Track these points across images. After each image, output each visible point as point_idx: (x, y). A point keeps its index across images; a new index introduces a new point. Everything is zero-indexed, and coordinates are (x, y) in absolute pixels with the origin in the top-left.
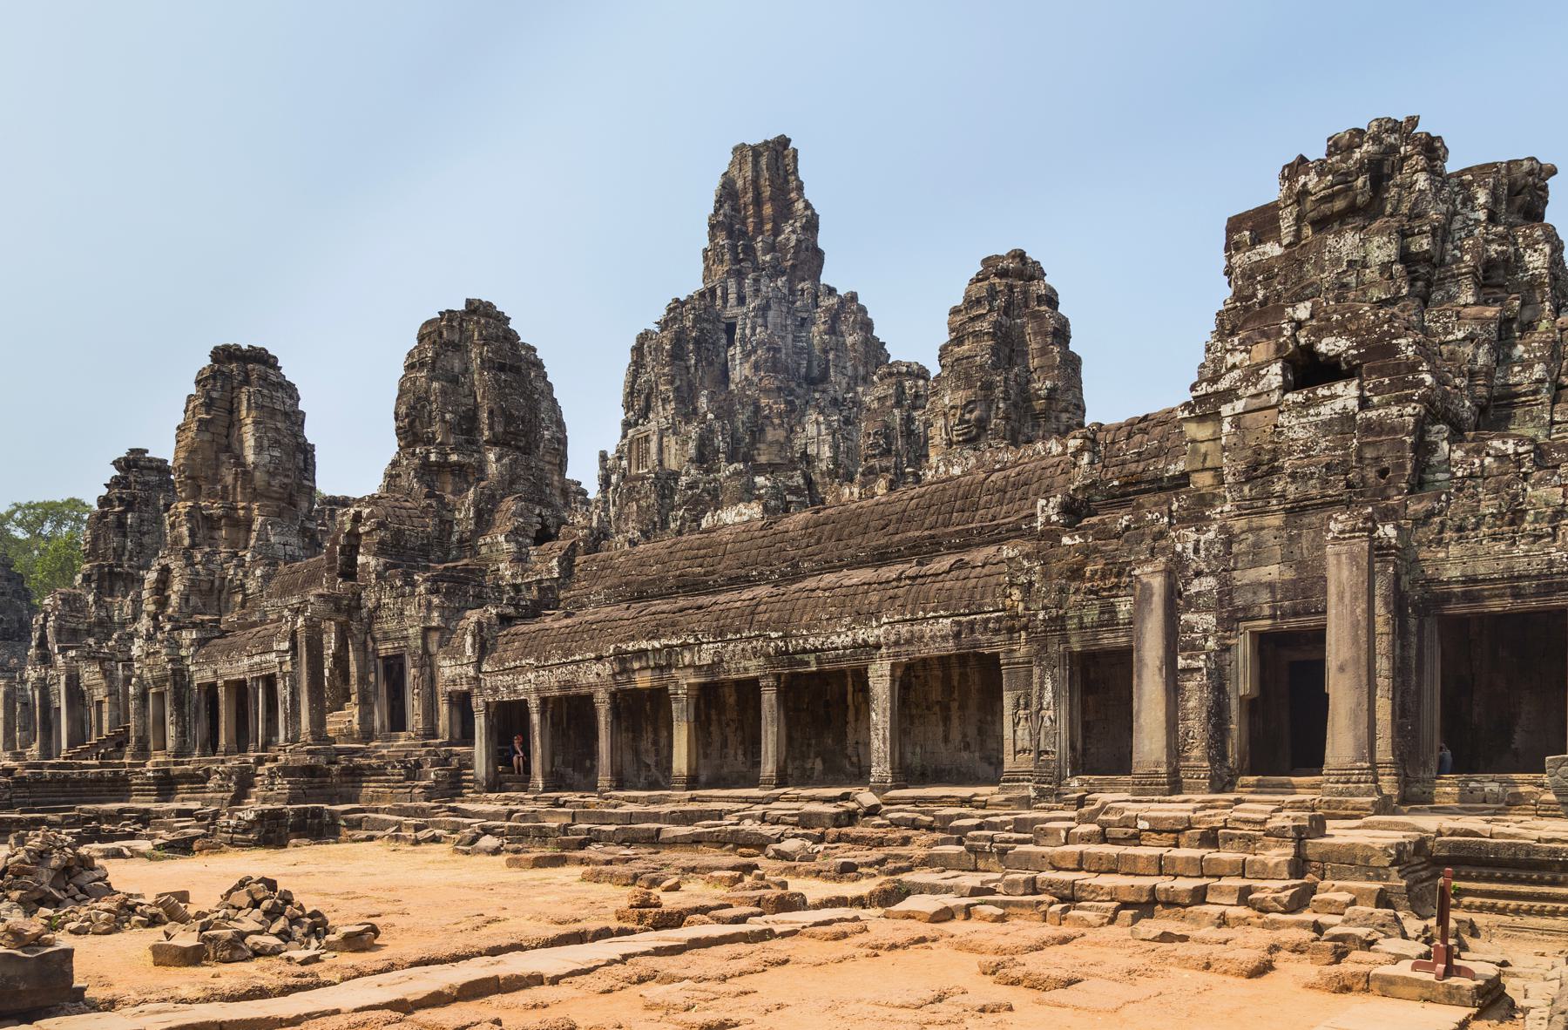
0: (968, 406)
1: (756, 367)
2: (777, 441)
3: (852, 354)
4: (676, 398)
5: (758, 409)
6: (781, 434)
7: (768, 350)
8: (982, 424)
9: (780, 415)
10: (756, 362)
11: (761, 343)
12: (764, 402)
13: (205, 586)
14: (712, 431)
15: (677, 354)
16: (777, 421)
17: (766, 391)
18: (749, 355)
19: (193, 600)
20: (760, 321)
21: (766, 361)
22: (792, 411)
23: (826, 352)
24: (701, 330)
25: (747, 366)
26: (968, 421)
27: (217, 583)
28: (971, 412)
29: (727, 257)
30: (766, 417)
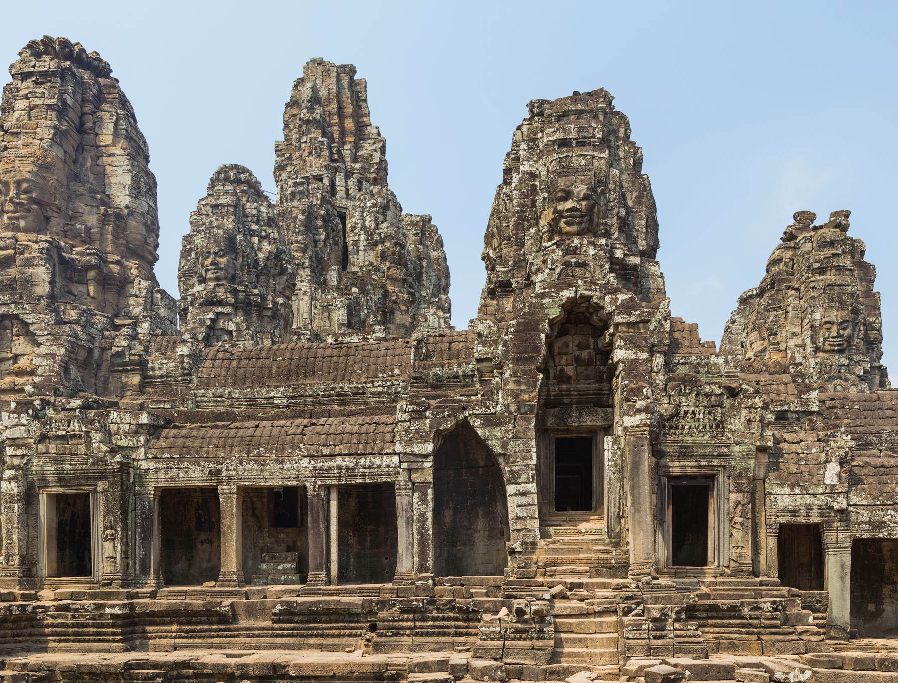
0: (842, 324)
1: (383, 256)
3: (435, 267)
4: (311, 266)
5: (386, 294)
6: (407, 320)
7: (396, 244)
8: (850, 338)
10: (383, 252)
11: (388, 237)
12: (390, 288)
13: (82, 355)
14: (358, 304)
15: (309, 227)
17: (393, 280)
18: (376, 244)
19: (74, 371)
20: (381, 217)
21: (393, 253)
22: (413, 302)
23: (420, 259)
24: (327, 211)
25: (372, 253)
26: (841, 336)
27: (96, 354)
28: (844, 329)
30: (395, 302)
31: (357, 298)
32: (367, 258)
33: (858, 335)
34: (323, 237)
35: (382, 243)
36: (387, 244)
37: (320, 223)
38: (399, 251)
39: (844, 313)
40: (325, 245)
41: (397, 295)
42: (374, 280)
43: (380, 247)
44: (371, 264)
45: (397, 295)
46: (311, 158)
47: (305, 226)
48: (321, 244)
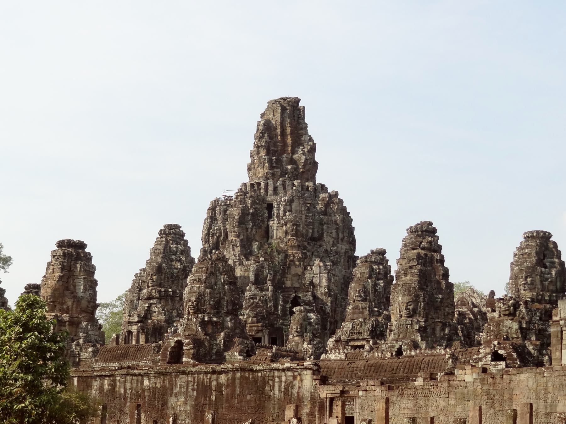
1: (286, 233)
2: (297, 275)
5: (287, 256)
7: (293, 225)
9: (300, 260)
12: (290, 252)
14: (262, 267)
16: (297, 263)
18: (282, 226)
20: (288, 208)
22: (306, 258)
24: (255, 209)
29: (267, 165)
30: (291, 261)
31: (262, 264)
32: (278, 234)
33: (420, 307)
34: (251, 226)
35: (286, 225)
36: (288, 225)
37: (250, 218)
38: (296, 229)
39: (410, 298)
40: (252, 230)
41: (294, 256)
42: (281, 247)
43: (284, 228)
44: (280, 238)
45: (294, 256)
46: (259, 168)
47: (239, 222)
48: (250, 230)
